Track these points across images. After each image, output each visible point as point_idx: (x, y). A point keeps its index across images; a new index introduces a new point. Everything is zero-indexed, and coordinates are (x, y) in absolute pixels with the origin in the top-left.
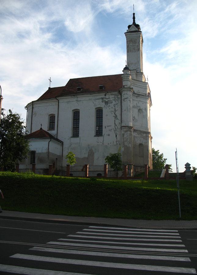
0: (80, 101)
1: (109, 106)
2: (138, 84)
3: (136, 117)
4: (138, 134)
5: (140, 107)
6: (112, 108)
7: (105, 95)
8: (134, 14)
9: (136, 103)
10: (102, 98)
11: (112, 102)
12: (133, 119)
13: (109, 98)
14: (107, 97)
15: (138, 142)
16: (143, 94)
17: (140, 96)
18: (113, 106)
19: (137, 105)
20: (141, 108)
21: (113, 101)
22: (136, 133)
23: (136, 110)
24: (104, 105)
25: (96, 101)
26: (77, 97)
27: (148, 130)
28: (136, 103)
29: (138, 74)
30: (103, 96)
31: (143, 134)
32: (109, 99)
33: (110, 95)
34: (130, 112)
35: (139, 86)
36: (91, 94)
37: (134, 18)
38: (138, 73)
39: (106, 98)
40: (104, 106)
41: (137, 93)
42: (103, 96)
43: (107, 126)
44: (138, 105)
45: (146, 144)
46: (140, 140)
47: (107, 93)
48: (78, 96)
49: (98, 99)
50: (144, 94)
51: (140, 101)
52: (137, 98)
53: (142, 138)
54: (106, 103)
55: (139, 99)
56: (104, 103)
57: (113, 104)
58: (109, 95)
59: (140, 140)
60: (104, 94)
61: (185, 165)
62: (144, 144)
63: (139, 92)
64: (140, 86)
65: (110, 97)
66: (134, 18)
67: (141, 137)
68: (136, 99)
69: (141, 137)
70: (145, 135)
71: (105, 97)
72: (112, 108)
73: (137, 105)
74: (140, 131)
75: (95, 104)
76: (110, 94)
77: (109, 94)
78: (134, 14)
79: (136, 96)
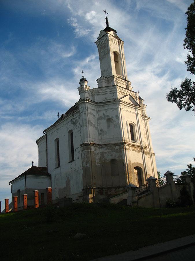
0: (59, 129)
1: (77, 126)
2: (103, 91)
3: (105, 129)
4: (108, 149)
5: (109, 116)
6: (79, 127)
7: (73, 115)
8: (107, 19)
9: (104, 113)
10: (72, 120)
11: (78, 121)
12: (100, 132)
13: (76, 118)
14: (75, 117)
15: (109, 158)
16: (111, 100)
17: (107, 104)
18: (79, 125)
19: (104, 115)
20: (110, 117)
21: (79, 119)
22: (105, 148)
23: (104, 122)
24: (73, 126)
25: (68, 124)
26: (56, 126)
27: (122, 140)
28: (104, 113)
29: (109, 79)
30: (72, 118)
31: (115, 147)
32: (76, 119)
33: (76, 114)
34: (87, 126)
35: (107, 93)
36: (64, 119)
37: (107, 22)
38: (109, 78)
39: (74, 119)
40: (74, 128)
41: (103, 101)
42: (72, 118)
43: (77, 149)
44: (106, 114)
45: (121, 158)
46: (112, 155)
47: (74, 113)
48: (56, 125)
49: (69, 122)
50: (113, 99)
51: (108, 109)
52: (104, 107)
53: (114, 152)
54: (74, 123)
55: (106, 107)
56: (73, 124)
57: (79, 123)
58: (75, 115)
59: (112, 155)
60: (72, 115)
61: (182, 173)
62: (117, 158)
63: (107, 100)
64: (106, 92)
65: (77, 116)
66: (107, 22)
67: (112, 151)
68: (103, 109)
69: (112, 151)
70: (117, 147)
71: (73, 118)
72: (79, 127)
73: (104, 115)
74: (109, 144)
75: (67, 128)
76: (75, 112)
77: (75, 114)
78: (107, 19)
79: (102, 105)
